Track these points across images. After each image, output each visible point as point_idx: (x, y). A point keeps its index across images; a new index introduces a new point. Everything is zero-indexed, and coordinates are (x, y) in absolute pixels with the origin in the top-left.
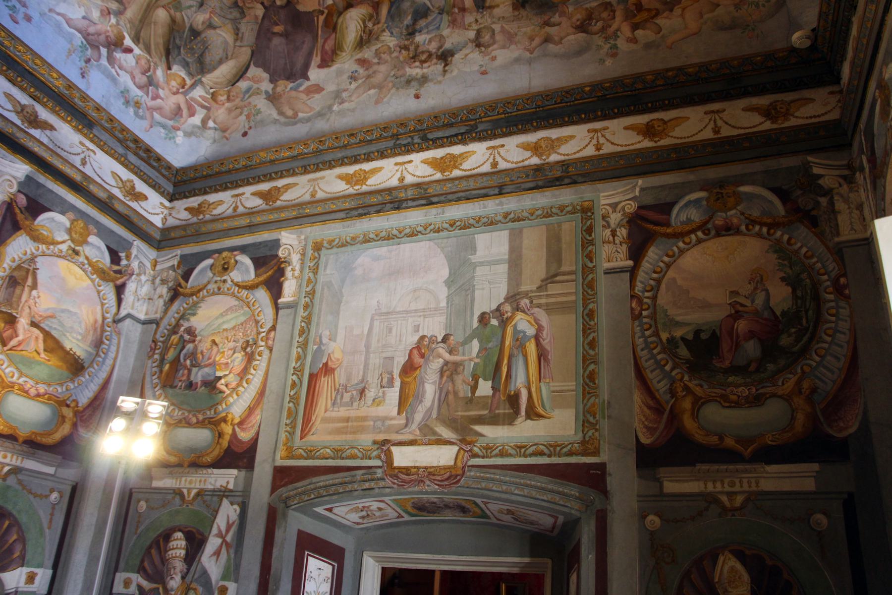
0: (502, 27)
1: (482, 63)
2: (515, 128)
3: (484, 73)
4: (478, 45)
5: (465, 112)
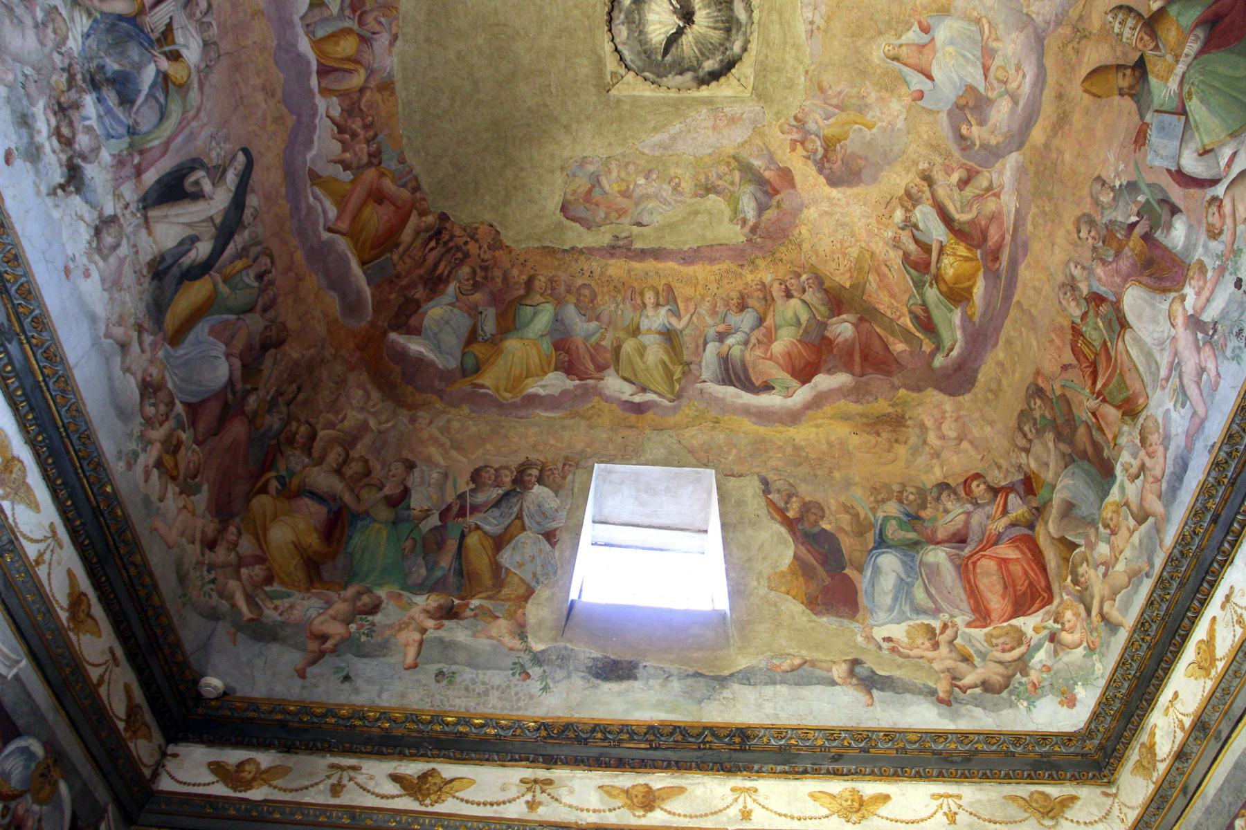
0: (126, 257)
1: (77, 256)
2: (27, 408)
3: (67, 271)
4: (98, 232)
5: (37, 312)
